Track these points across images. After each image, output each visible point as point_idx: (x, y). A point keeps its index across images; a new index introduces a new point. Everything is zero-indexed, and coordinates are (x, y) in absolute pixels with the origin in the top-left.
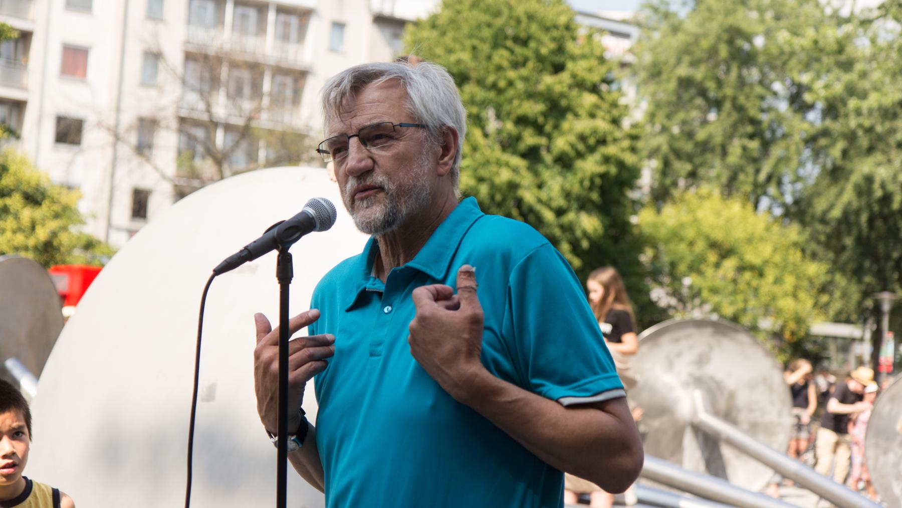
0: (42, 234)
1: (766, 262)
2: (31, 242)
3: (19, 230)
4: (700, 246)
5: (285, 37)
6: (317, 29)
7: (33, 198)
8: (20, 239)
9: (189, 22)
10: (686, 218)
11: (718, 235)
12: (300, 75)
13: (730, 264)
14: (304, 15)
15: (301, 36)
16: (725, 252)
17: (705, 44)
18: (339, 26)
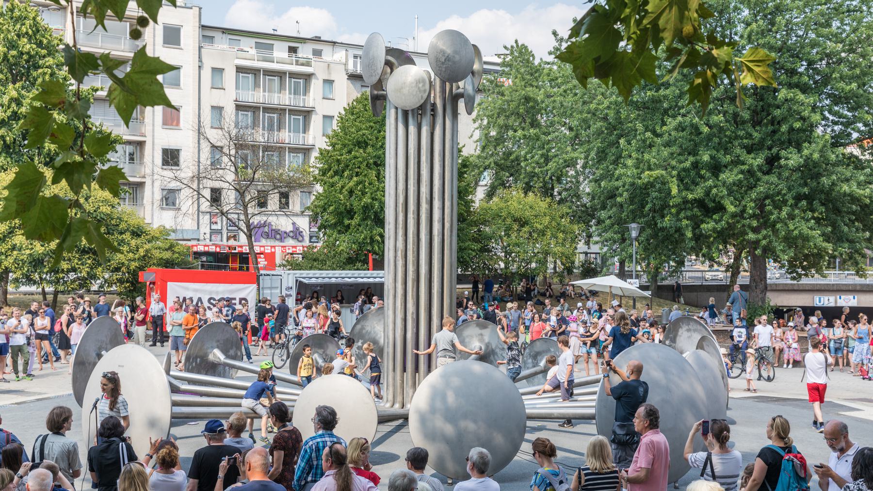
0: (142, 252)
1: (547, 227)
2: (137, 256)
3: (131, 251)
4: (509, 221)
5: (271, 128)
6: (316, 86)
7: (137, 233)
8: (131, 255)
9: (237, 88)
10: (502, 205)
11: (517, 215)
12: (307, 114)
13: (526, 229)
14: (308, 77)
15: (306, 91)
16: (522, 223)
17: (513, 105)
18: (329, 82)
